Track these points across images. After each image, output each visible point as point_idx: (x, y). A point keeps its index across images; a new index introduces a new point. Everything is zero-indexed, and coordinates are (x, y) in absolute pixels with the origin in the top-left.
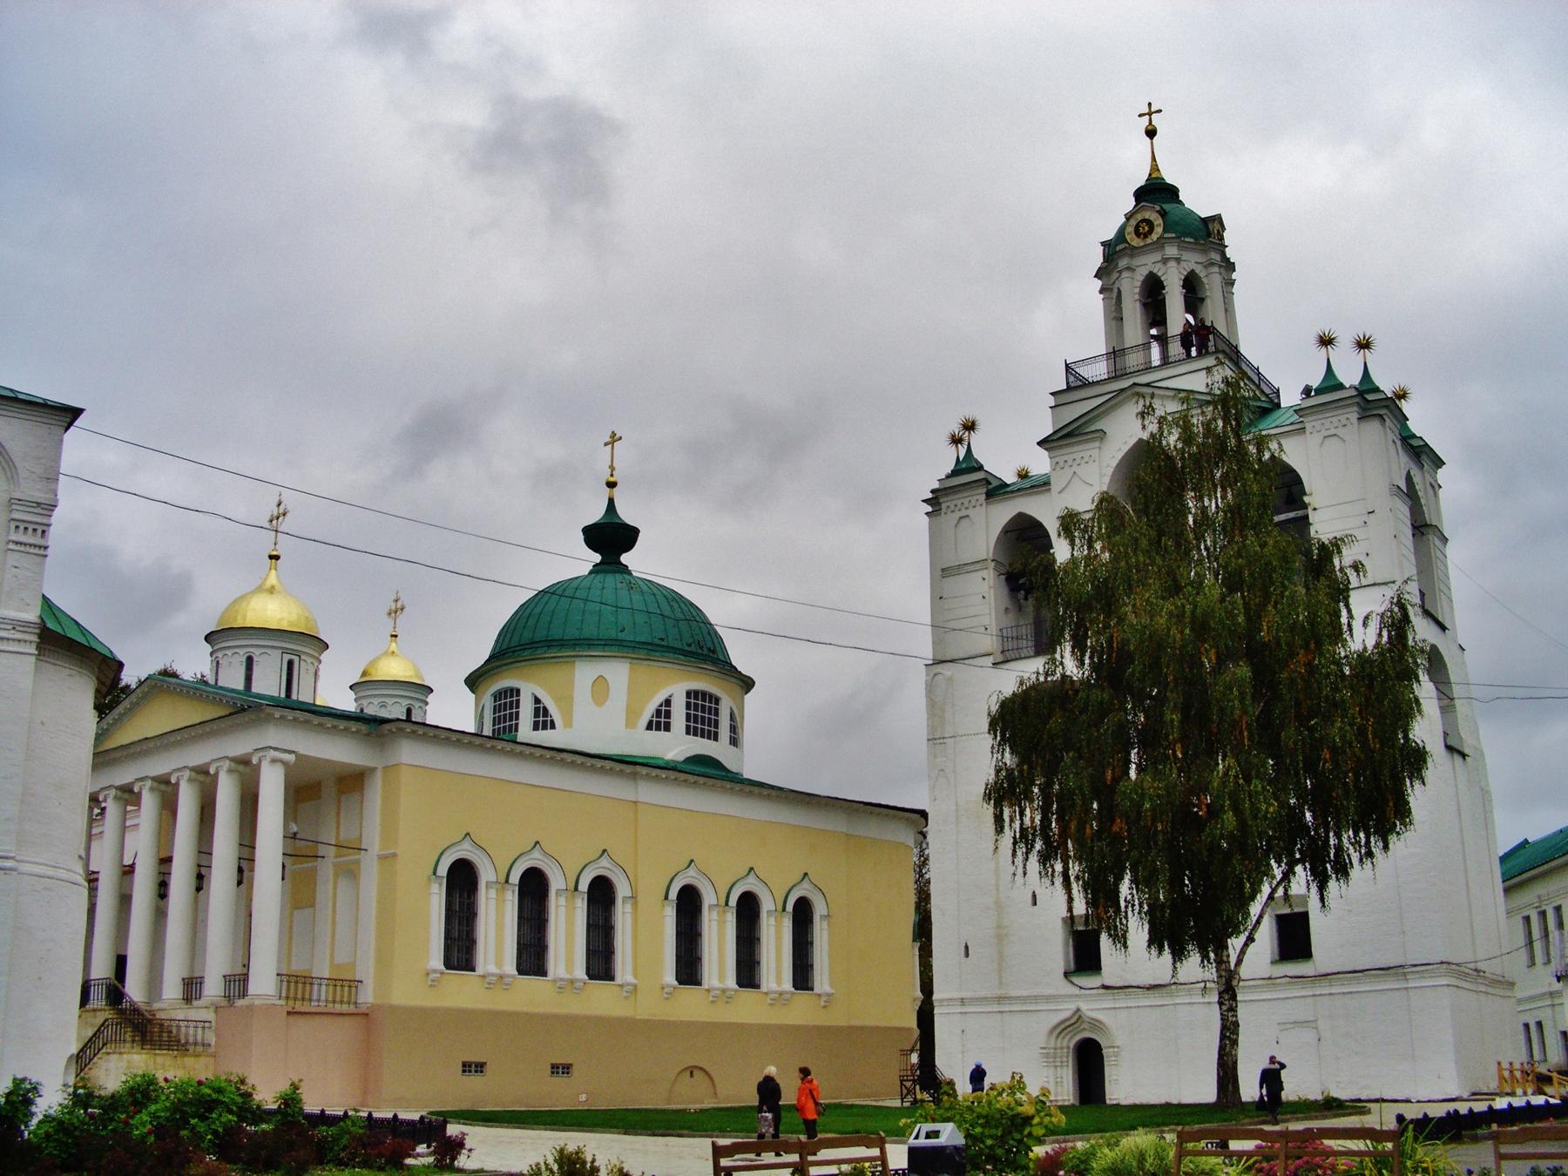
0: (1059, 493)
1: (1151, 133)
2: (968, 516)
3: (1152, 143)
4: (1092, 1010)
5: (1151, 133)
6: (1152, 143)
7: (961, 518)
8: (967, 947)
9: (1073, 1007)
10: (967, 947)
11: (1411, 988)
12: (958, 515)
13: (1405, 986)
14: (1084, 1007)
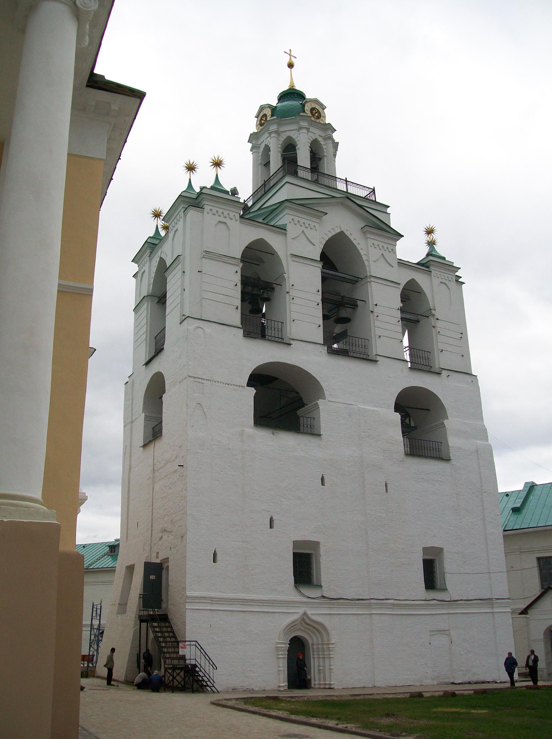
0: (293, 239)
1: (291, 66)
2: (225, 223)
3: (291, 71)
4: (315, 614)
5: (291, 66)
6: (291, 71)
7: (220, 222)
8: (215, 555)
9: (301, 611)
10: (215, 555)
11: (496, 612)
12: (217, 219)
13: (492, 611)
14: (309, 612)
